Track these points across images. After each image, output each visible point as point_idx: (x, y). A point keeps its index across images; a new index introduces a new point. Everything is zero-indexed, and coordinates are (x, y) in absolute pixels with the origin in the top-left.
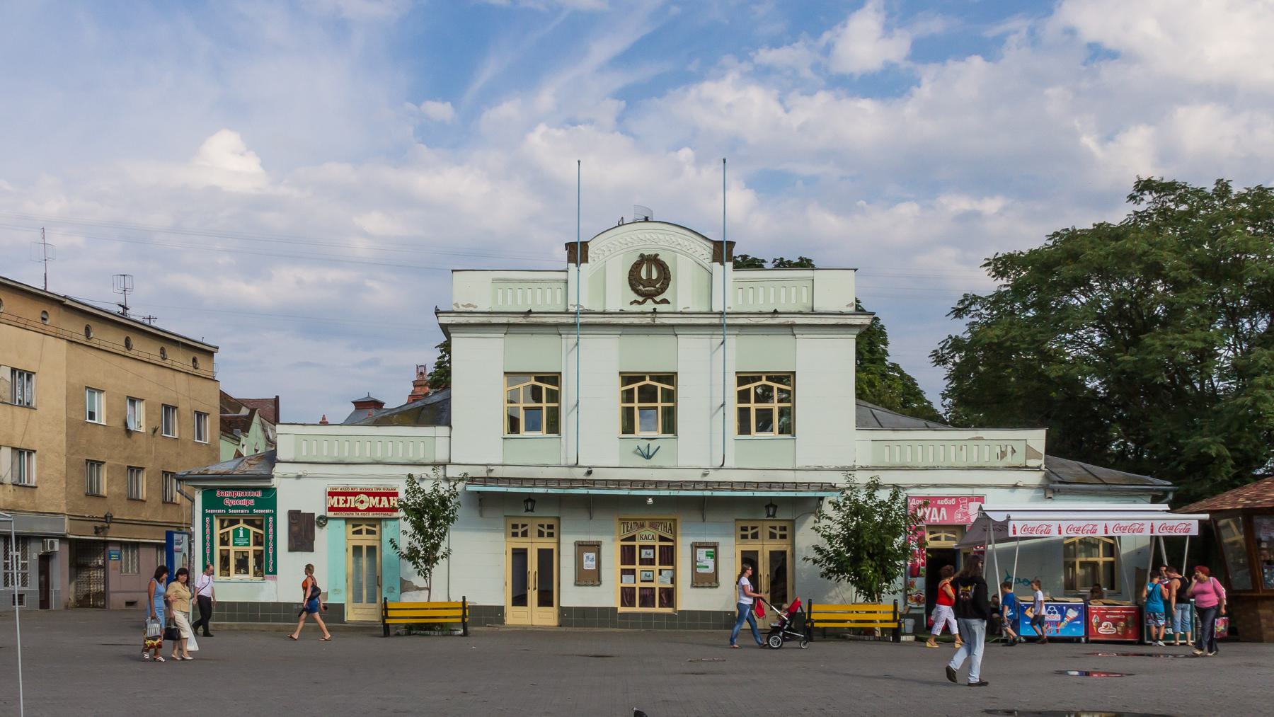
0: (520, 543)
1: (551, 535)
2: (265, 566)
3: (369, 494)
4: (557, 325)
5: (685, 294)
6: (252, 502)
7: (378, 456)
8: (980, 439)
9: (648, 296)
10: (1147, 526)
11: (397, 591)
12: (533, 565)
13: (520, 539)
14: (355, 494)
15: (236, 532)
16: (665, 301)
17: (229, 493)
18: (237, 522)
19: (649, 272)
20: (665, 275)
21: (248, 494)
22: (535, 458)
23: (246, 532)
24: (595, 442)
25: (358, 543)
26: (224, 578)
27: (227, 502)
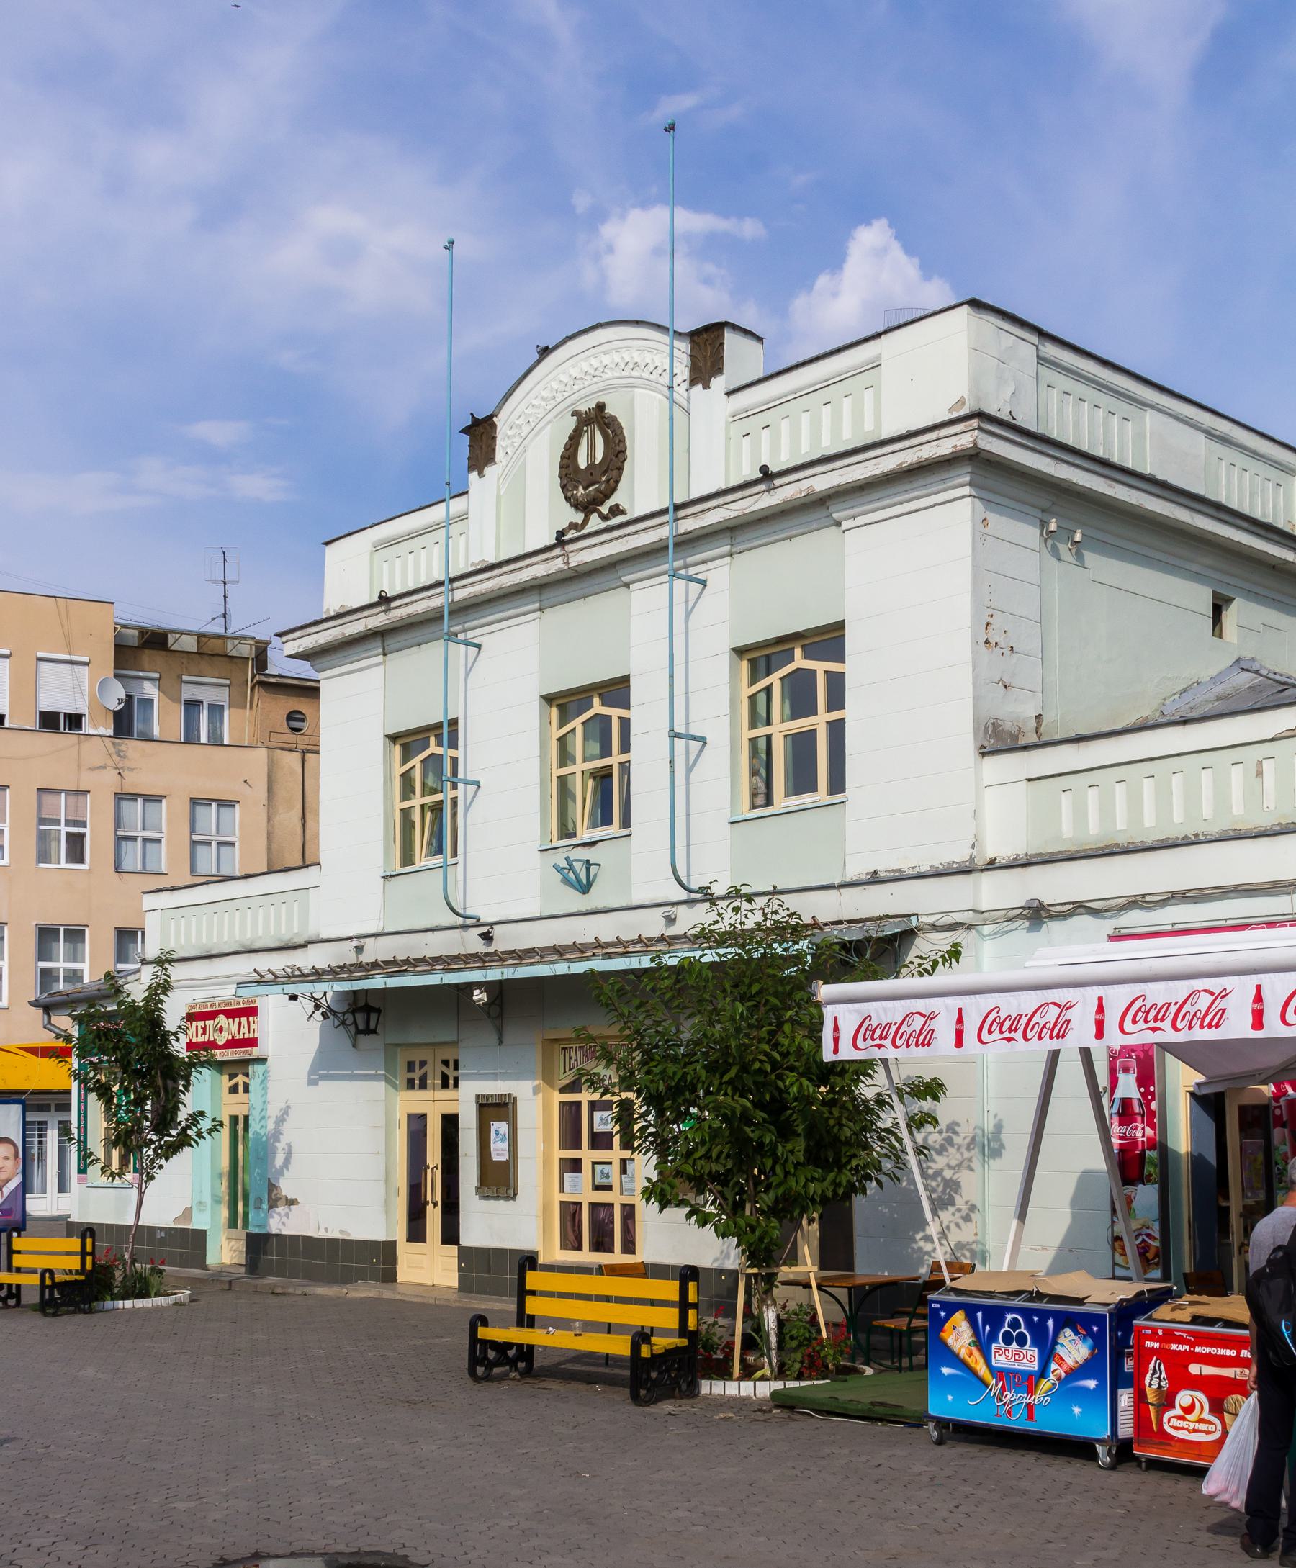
3: (231, 1014)
5: (641, 489)
10: (1242, 990)
14: (212, 1015)
16: (616, 511)
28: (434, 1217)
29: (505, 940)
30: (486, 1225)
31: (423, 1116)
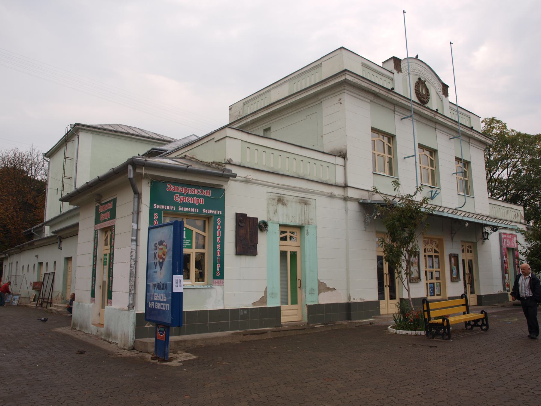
6: (201, 201)
7: (301, 173)
11: (316, 292)
17: (180, 189)
21: (198, 191)
25: (284, 249)
28: (387, 290)
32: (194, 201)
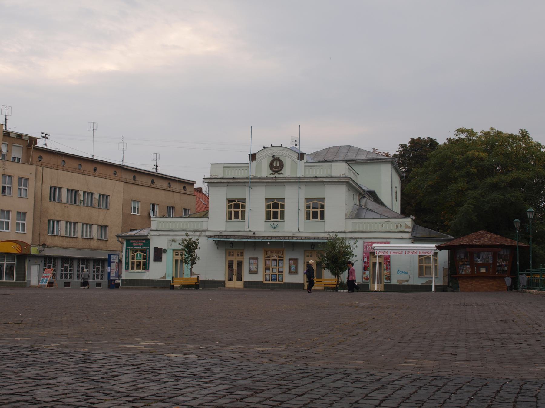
0: (231, 258)
1: (242, 256)
2: (146, 266)
4: (244, 182)
5: (287, 172)
8: (389, 221)
9: (275, 172)
12: (235, 266)
13: (231, 257)
15: (137, 255)
16: (281, 173)
18: (137, 251)
19: (276, 163)
20: (282, 165)
21: (141, 241)
22: (237, 228)
23: (140, 255)
24: (256, 223)
26: (132, 271)
27: (134, 244)
29: (257, 234)
30: (247, 277)
31: (233, 261)
32: (140, 244)
